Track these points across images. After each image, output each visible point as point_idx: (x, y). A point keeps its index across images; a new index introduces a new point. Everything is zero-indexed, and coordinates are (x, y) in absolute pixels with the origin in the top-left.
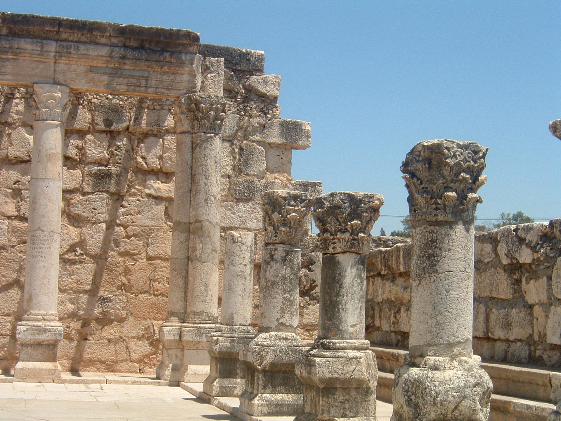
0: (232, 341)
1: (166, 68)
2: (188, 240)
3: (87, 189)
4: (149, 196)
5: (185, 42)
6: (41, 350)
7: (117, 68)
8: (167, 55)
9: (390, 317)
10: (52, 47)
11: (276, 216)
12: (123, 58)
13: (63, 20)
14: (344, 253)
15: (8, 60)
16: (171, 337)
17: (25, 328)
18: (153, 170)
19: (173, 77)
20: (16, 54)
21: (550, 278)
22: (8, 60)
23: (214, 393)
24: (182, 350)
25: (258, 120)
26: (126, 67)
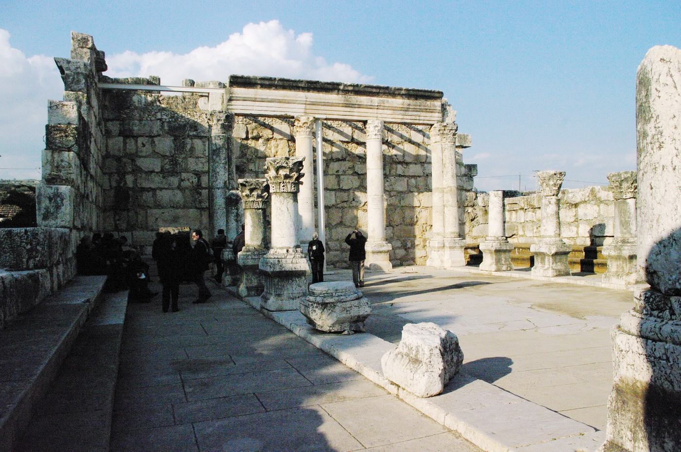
0: (500, 245)
4: (400, 176)
9: (533, 230)
10: (376, 100)
16: (440, 245)
19: (430, 114)
22: (355, 107)
23: (494, 270)
24: (444, 251)
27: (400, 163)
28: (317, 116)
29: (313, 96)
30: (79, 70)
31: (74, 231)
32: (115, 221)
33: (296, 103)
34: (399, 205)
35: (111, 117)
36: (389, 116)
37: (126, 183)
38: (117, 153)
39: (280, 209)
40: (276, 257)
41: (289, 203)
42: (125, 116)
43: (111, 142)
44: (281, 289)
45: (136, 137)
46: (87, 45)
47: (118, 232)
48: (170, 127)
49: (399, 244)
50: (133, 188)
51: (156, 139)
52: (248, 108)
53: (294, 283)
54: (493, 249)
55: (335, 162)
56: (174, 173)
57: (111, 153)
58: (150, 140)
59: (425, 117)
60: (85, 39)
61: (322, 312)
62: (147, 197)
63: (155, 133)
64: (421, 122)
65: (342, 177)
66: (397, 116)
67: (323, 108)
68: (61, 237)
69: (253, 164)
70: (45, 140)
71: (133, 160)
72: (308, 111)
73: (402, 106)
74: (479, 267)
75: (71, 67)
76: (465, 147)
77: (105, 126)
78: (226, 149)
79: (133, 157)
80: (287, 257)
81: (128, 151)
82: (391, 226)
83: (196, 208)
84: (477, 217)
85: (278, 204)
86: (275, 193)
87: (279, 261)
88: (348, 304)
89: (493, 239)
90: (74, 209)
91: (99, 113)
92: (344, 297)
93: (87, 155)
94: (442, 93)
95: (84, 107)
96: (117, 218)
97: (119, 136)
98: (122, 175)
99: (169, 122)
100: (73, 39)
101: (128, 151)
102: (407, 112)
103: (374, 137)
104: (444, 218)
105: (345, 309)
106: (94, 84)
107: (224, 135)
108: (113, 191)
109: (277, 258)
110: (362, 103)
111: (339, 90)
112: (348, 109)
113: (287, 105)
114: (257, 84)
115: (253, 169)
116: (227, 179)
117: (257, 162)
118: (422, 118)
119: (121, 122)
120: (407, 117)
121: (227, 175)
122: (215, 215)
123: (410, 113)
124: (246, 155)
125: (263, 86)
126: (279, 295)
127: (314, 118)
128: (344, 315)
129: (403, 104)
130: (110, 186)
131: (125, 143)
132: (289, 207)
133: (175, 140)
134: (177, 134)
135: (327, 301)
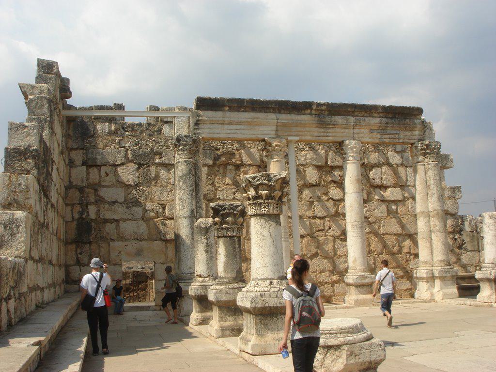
1: (408, 128)
5: (416, 113)
6: (365, 288)
7: (384, 129)
8: (408, 120)
10: (352, 119)
12: (387, 123)
13: (357, 105)
15: (330, 128)
16: (429, 276)
17: (356, 277)
18: (378, 186)
20: (334, 125)
22: (330, 128)
26: (389, 128)
28: (290, 138)
29: (285, 117)
30: (43, 95)
31: (30, 263)
32: (77, 255)
33: (267, 125)
35: (75, 147)
37: (88, 215)
38: (80, 183)
39: (261, 234)
40: (258, 290)
41: (272, 227)
42: (88, 145)
43: (74, 171)
45: (99, 167)
46: (52, 71)
47: (80, 266)
48: (134, 155)
50: (96, 219)
52: (217, 131)
53: (280, 320)
55: (308, 187)
57: (74, 183)
58: (114, 169)
59: (404, 135)
60: (50, 65)
61: (324, 358)
62: (110, 228)
63: (119, 162)
64: (401, 141)
66: (374, 136)
67: (294, 129)
68: (14, 268)
69: (221, 193)
70: (4, 164)
71: (96, 190)
72: (279, 133)
73: (380, 125)
74: (476, 298)
75: (35, 92)
77: (69, 155)
78: (193, 175)
80: (271, 291)
81: (91, 181)
83: (161, 240)
84: (465, 243)
85: (259, 229)
86: (255, 215)
87: (261, 295)
90: (31, 237)
91: (62, 141)
92: (351, 338)
93: (48, 182)
95: (46, 133)
96: (79, 251)
97: (83, 165)
98: (84, 205)
100: (38, 65)
102: (385, 131)
106: (58, 111)
107: (191, 160)
108: (75, 223)
109: (259, 292)
110: (337, 123)
111: (312, 109)
112: (323, 130)
114: (226, 106)
115: (222, 198)
116: (194, 207)
119: (85, 151)
121: (194, 203)
122: (182, 246)
123: (388, 132)
125: (231, 109)
128: (352, 361)
129: (380, 123)
130: (73, 217)
131: (88, 173)
132: (271, 231)
133: (139, 168)
134: (142, 163)
135: (330, 344)
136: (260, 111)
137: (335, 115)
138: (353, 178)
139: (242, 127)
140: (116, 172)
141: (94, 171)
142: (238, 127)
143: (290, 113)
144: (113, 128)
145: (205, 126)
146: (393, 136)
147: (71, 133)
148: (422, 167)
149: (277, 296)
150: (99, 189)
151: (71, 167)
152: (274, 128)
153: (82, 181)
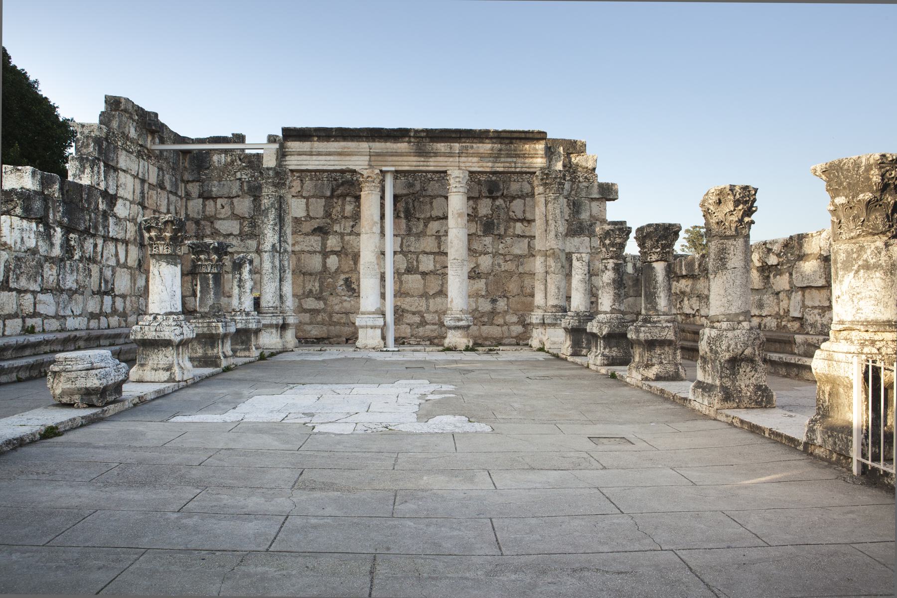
0: (580, 322)
2: (546, 261)
3: (480, 233)
4: (518, 236)
8: (527, 146)
10: (457, 146)
11: (607, 242)
14: (657, 261)
21: (791, 274)
25: (584, 184)
27: (519, 220)
28: (384, 169)
29: (378, 146)
34: (516, 271)
36: (475, 164)
38: (196, 216)
43: (191, 204)
44: (146, 358)
45: (215, 199)
48: (250, 189)
49: (515, 319)
51: (235, 200)
52: (305, 163)
54: (570, 327)
56: (253, 235)
57: (191, 216)
63: (234, 193)
64: (518, 170)
65: (443, 238)
66: (485, 164)
71: (212, 223)
72: (373, 163)
76: (614, 200)
77: (185, 188)
79: (211, 219)
81: (207, 213)
82: (504, 296)
88: (74, 375)
89: (572, 314)
94: (545, 133)
99: (248, 182)
101: (207, 213)
103: (455, 190)
104: (546, 288)
105: (69, 379)
111: (410, 137)
112: (423, 159)
113: (348, 158)
117: (343, 223)
118: (519, 165)
120: (499, 165)
121: (277, 237)
123: (502, 160)
124: (331, 215)
126: (142, 365)
127: (381, 171)
129: (492, 150)
131: (204, 206)
133: (254, 200)
136: (352, 141)
137: (437, 142)
138: (455, 212)
139: (332, 158)
140: (232, 203)
141: (210, 203)
142: (328, 158)
143: (386, 142)
144: (229, 159)
145: (293, 158)
146: (508, 165)
147: (187, 164)
148: (543, 200)
149: (156, 330)
150: (215, 221)
151: (187, 199)
152: (367, 158)
153: (198, 213)
